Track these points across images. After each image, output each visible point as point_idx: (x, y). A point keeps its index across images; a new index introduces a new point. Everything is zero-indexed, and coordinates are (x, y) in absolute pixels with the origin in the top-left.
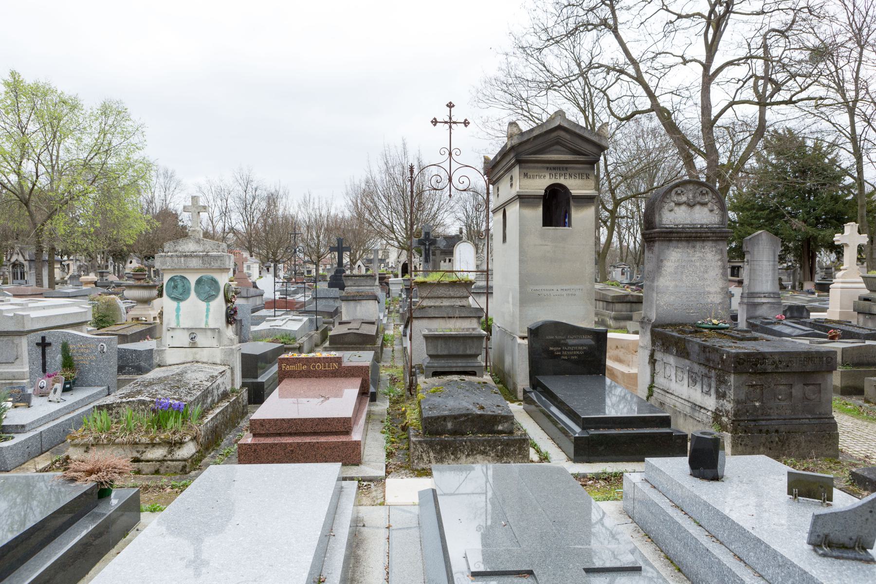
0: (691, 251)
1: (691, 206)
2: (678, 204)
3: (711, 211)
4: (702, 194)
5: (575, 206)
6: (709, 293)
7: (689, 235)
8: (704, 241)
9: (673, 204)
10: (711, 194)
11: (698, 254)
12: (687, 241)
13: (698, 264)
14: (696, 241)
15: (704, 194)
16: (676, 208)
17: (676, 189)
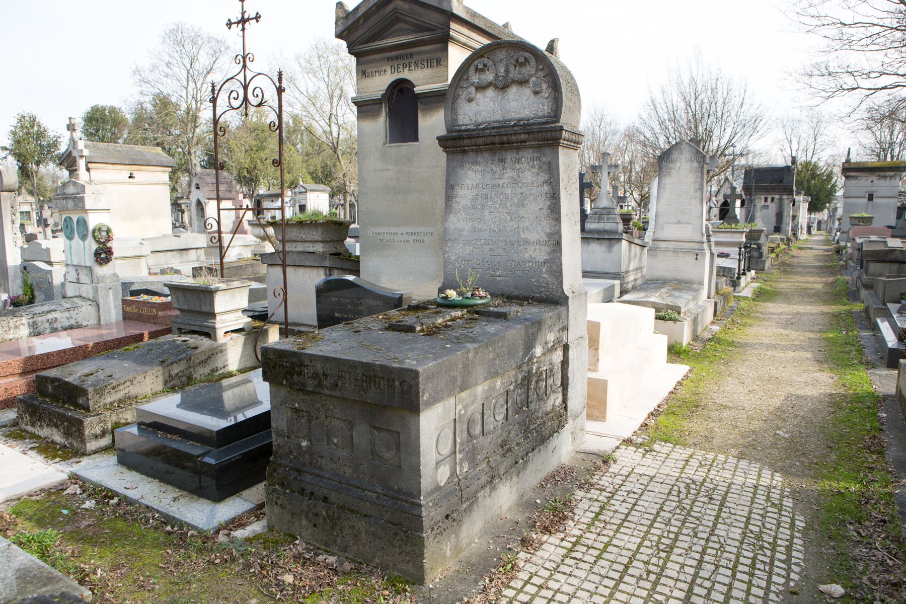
0: (497, 168)
1: (502, 86)
2: (481, 88)
3: (536, 93)
4: (519, 64)
5: (423, 110)
6: (527, 242)
7: (489, 140)
8: (518, 149)
9: (472, 89)
10: (533, 62)
11: (509, 173)
12: (491, 150)
13: (508, 191)
14: (506, 150)
15: (522, 65)
16: (479, 96)
17: (475, 63)
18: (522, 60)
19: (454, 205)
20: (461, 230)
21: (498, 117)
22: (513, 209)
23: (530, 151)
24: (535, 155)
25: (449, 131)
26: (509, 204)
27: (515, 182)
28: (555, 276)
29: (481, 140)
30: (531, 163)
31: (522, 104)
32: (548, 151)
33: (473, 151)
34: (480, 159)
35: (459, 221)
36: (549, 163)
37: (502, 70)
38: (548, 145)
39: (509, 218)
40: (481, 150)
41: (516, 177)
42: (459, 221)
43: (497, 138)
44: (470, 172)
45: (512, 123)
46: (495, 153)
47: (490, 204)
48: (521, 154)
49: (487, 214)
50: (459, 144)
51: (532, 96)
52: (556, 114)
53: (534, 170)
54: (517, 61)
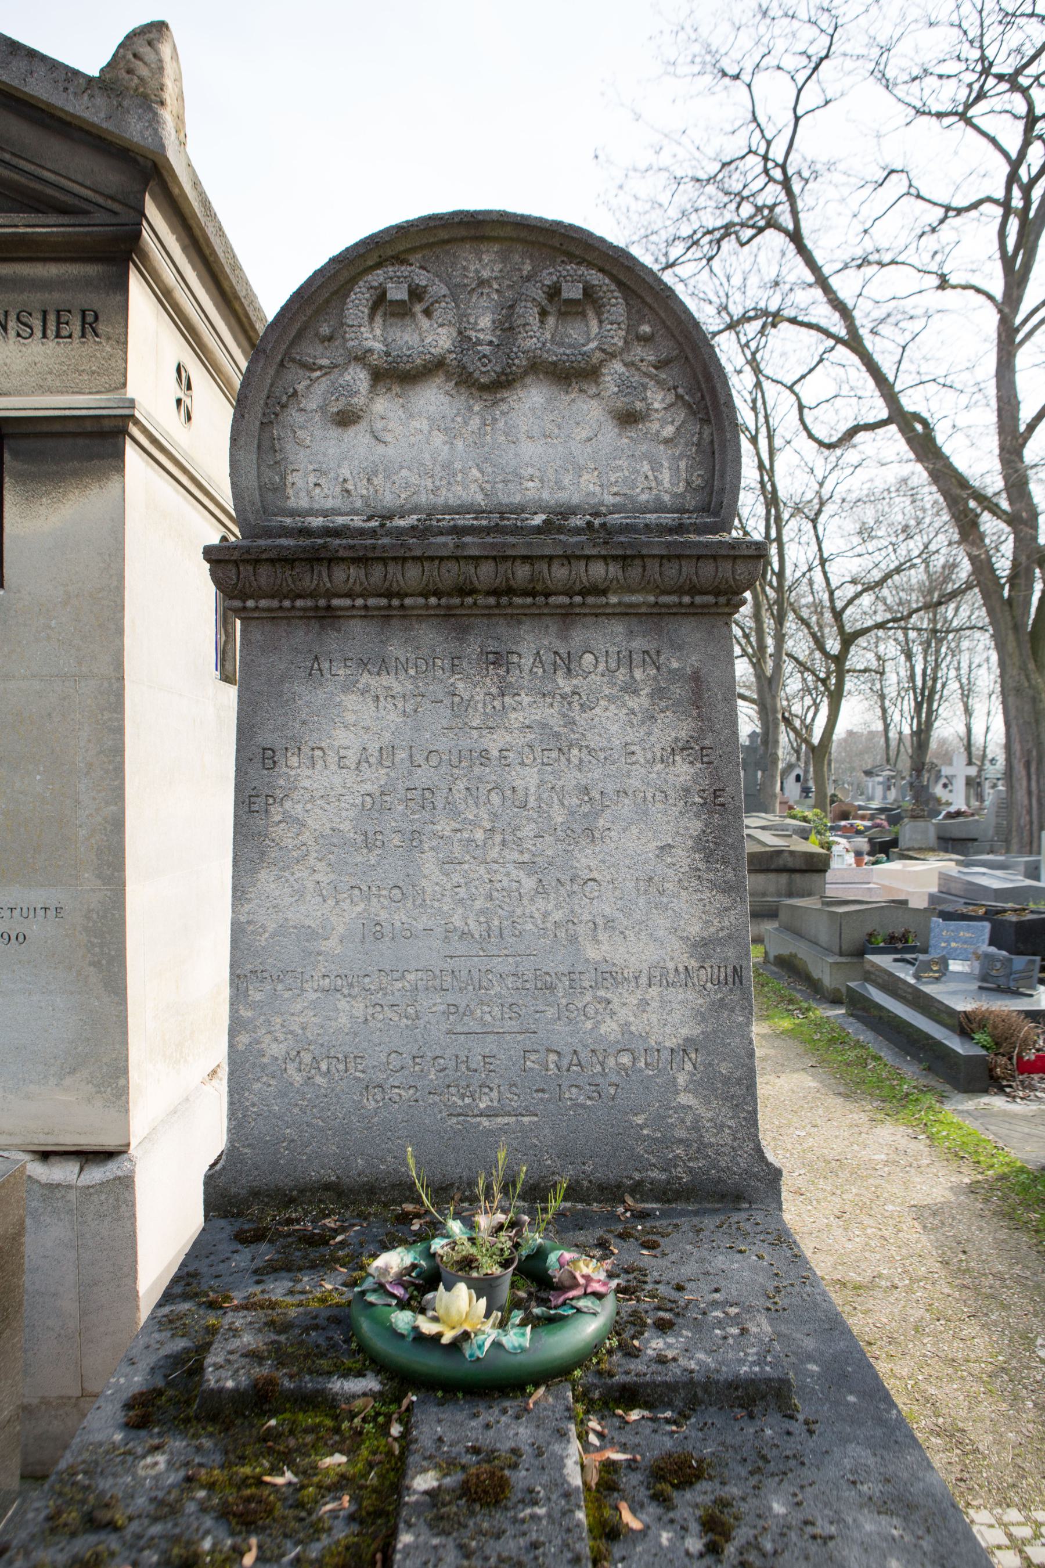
0: (475, 688)
1: (486, 380)
2: (396, 375)
3: (628, 418)
4: (558, 305)
5: (22, 478)
6: (609, 976)
7: (450, 574)
8: (567, 617)
9: (358, 377)
10: (617, 308)
11: (529, 710)
12: (448, 615)
13: (527, 778)
14: (516, 618)
15: (571, 310)
16: (381, 405)
17: (377, 277)
18: (572, 292)
19: (276, 832)
20: (312, 935)
21: (468, 491)
22: (549, 848)
23: (618, 628)
24: (638, 643)
25: (249, 530)
26: (528, 831)
27: (558, 744)
28: (728, 1098)
29: (413, 572)
30: (622, 675)
31: (566, 454)
32: (689, 631)
33: (367, 614)
34: (396, 650)
35: (300, 894)
36: (696, 677)
37: (485, 321)
38: (695, 612)
39: (529, 883)
40: (405, 614)
41: (556, 723)
42: (300, 894)
43: (487, 570)
44: (351, 700)
45: (538, 520)
46: (465, 630)
47: (444, 826)
48: (579, 636)
49: (429, 864)
50: (308, 583)
51: (610, 434)
52: (715, 495)
53: (633, 703)
54: (554, 293)
